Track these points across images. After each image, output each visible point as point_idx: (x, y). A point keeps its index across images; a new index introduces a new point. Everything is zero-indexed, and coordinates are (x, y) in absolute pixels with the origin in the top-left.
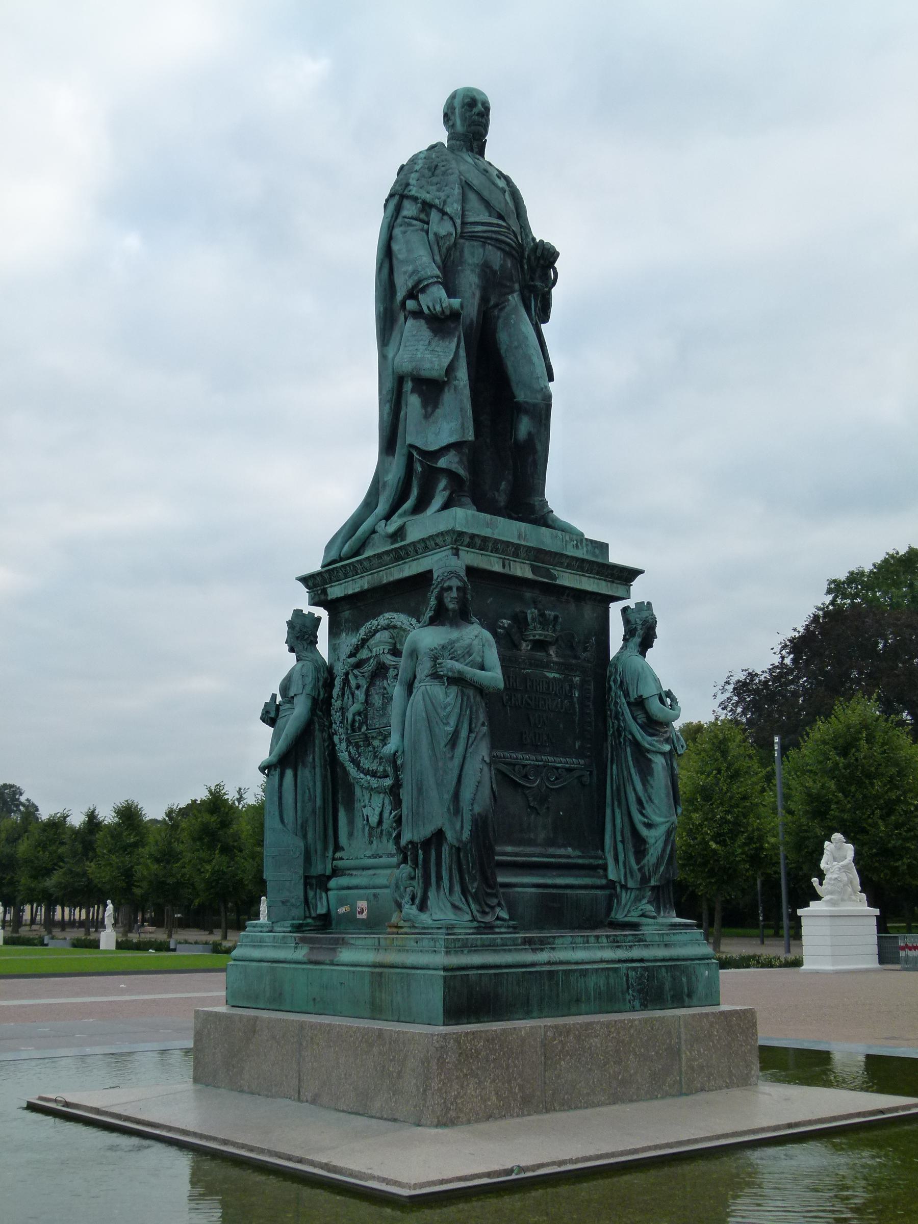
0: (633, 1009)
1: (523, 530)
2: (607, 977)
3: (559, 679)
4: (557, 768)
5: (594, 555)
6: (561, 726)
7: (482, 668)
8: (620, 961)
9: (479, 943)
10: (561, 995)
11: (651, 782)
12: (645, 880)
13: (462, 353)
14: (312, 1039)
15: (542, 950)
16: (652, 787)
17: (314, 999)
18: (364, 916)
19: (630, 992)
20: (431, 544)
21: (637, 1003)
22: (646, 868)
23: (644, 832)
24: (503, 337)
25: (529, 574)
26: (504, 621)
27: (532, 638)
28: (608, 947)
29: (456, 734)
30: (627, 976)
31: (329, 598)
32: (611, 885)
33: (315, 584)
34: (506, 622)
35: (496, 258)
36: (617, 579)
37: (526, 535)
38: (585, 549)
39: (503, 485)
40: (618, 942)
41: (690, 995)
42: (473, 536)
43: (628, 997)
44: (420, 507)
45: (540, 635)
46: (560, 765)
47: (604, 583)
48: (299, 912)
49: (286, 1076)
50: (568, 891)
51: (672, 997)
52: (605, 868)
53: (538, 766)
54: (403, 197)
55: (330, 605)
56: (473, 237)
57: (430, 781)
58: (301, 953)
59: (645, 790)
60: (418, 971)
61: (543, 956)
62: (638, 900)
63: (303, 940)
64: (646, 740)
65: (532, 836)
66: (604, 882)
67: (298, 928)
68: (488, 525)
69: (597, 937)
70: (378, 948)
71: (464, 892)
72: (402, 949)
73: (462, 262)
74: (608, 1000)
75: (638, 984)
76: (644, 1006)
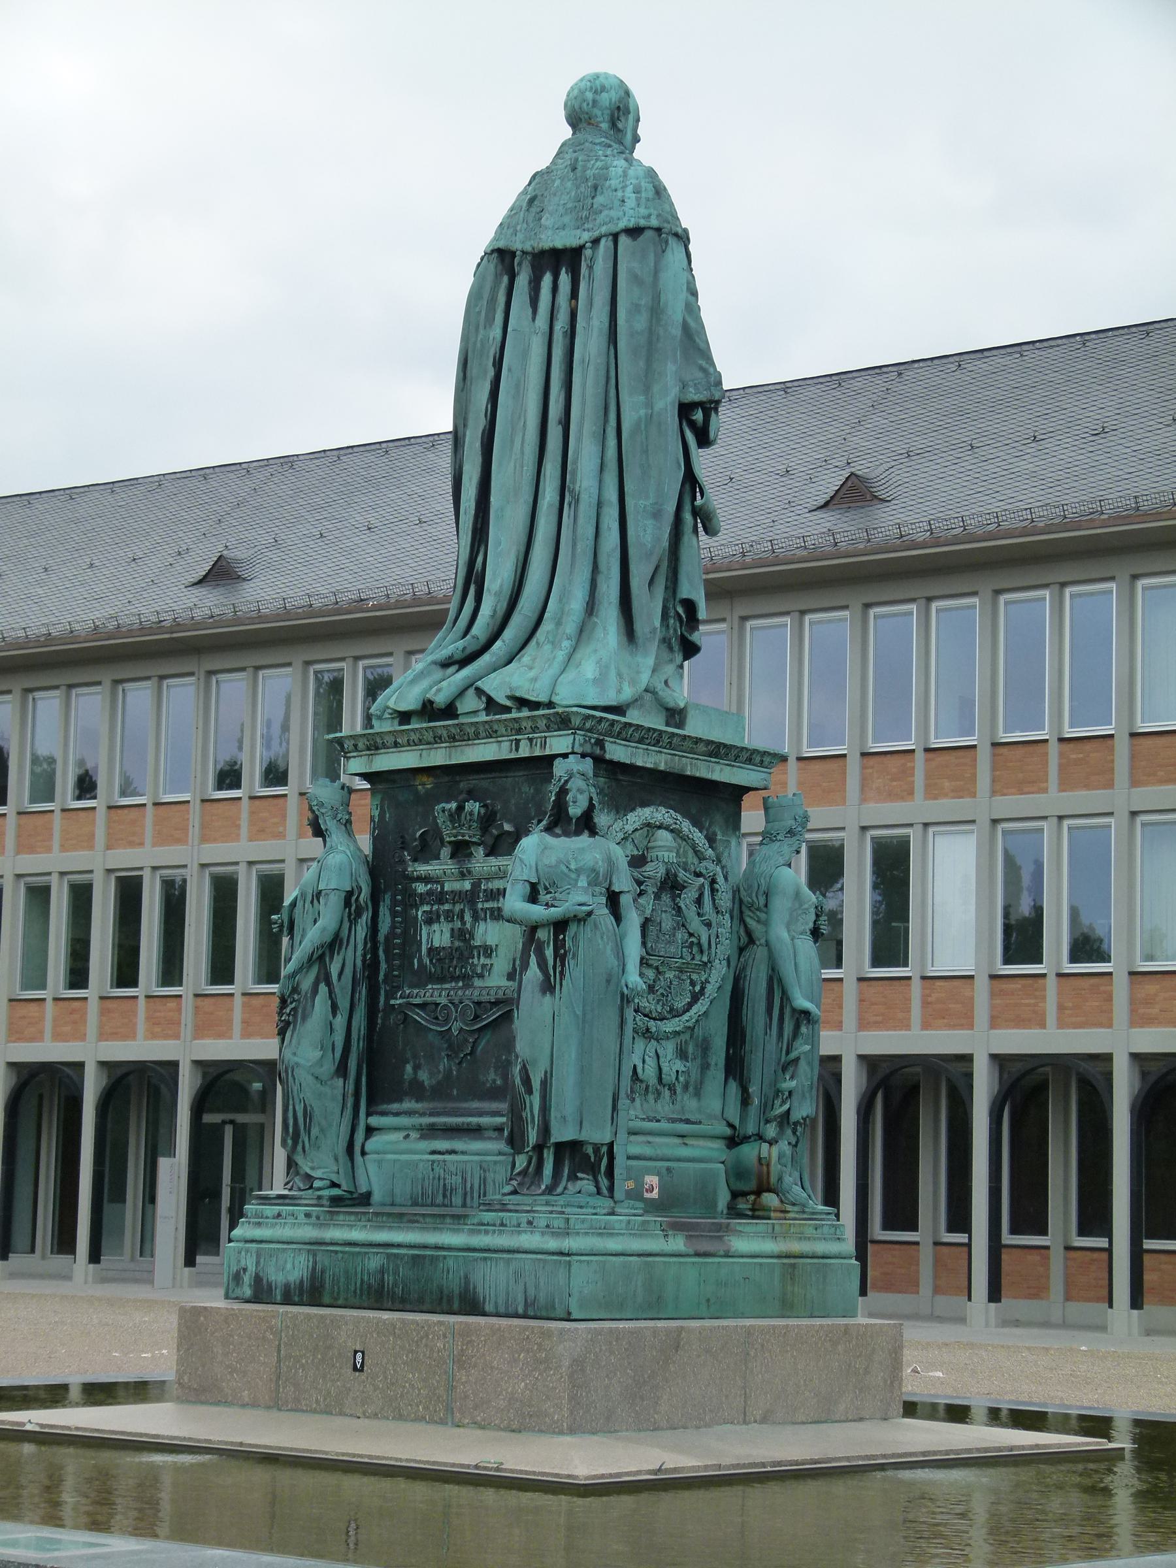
14: (763, 1346)
17: (708, 1300)
18: (655, 1194)
20: (758, 759)
31: (608, 757)
49: (727, 1396)
58: (678, 1243)
60: (832, 1261)
63: (677, 1227)
72: (802, 1238)
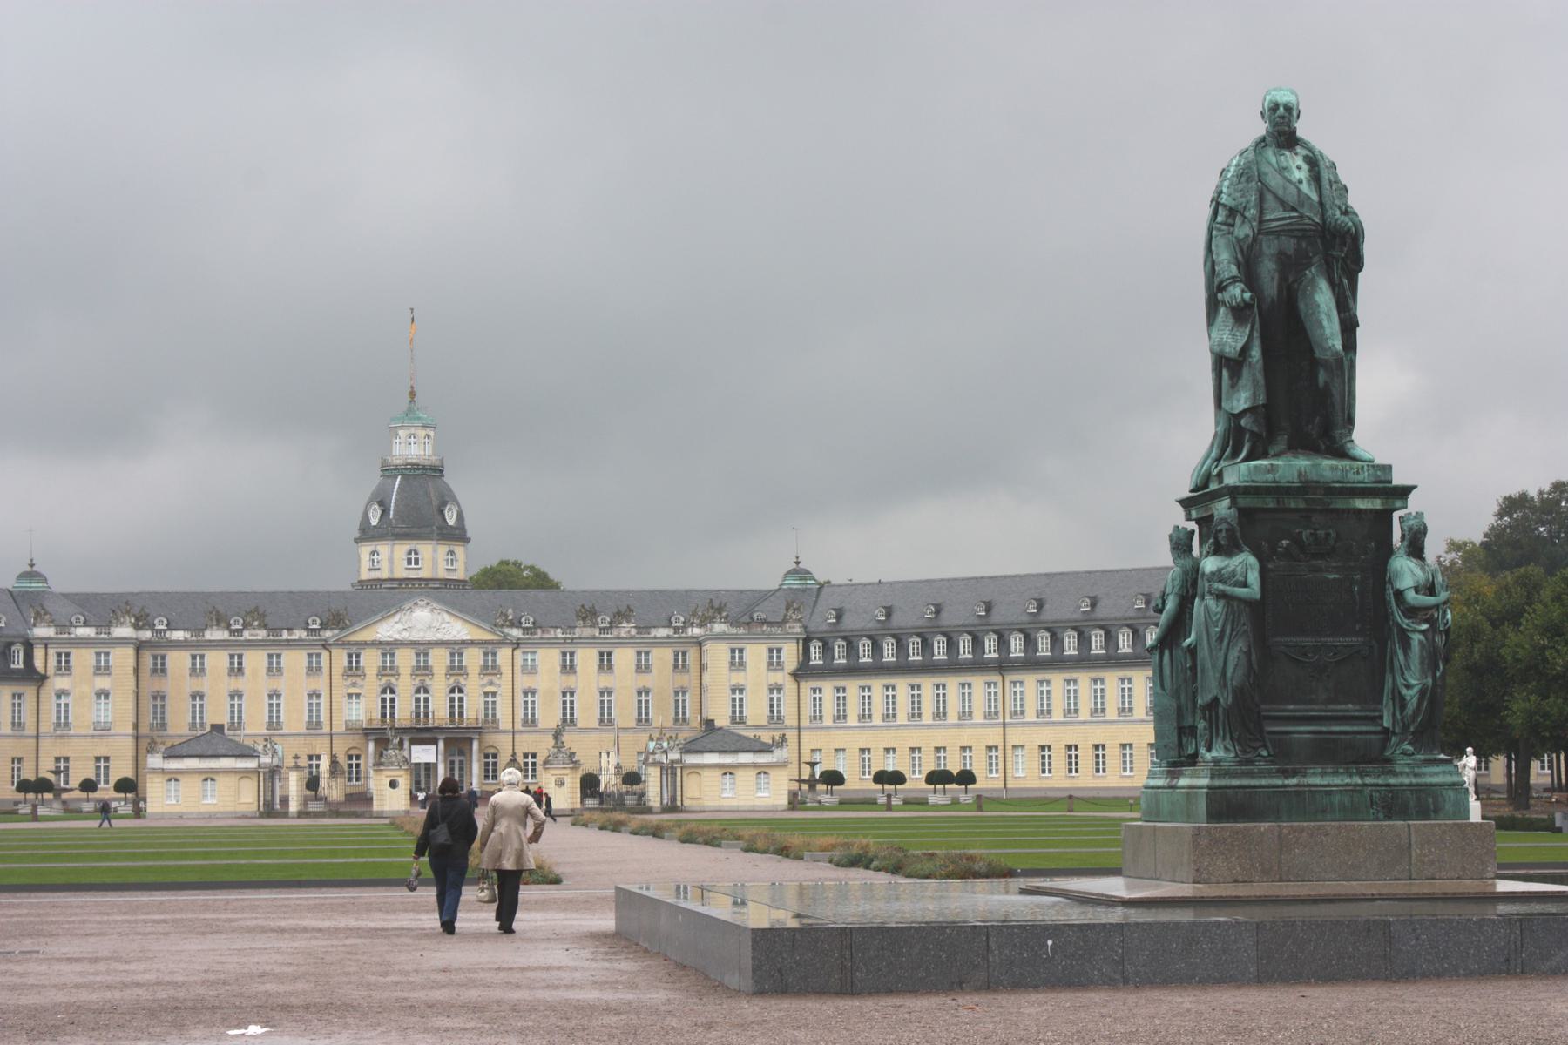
7: (1245, 585)
12: (1405, 728)
13: (1256, 334)
21: (1381, 816)
23: (1404, 691)
24: (1302, 306)
29: (1223, 632)
32: (1386, 731)
33: (1186, 503)
35: (1289, 245)
39: (1317, 420)
41: (1436, 811)
44: (1235, 454)
48: (1174, 753)
52: (1381, 717)
54: (1218, 204)
55: (1198, 521)
56: (1270, 232)
57: (1209, 665)
62: (1401, 742)
64: (1405, 623)
67: (1174, 764)
70: (1191, 776)
71: (1232, 739)
73: (1261, 253)
74: (1352, 812)
76: (1389, 818)
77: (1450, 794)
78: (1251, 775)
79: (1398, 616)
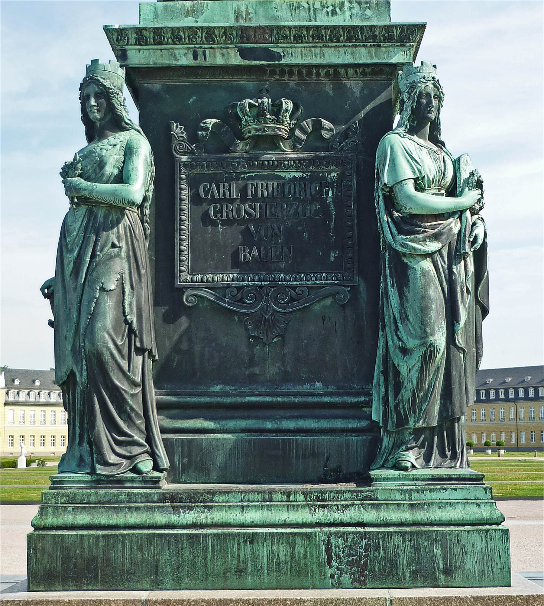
0: (340, 586)
1: (243, 9)
2: (293, 545)
3: (301, 178)
4: (294, 288)
5: (365, 17)
6: (306, 235)
8: (319, 525)
9: (92, 498)
10: (210, 563)
11: (407, 294)
15: (190, 509)
16: (407, 300)
19: (334, 563)
21: (346, 579)
22: (401, 405)
25: (236, 60)
26: (208, 121)
27: (248, 135)
28: (304, 506)
30: (329, 543)
34: (211, 122)
36: (384, 41)
37: (248, 13)
38: (348, 14)
40: (324, 500)
41: (448, 572)
42: (139, 31)
43: (329, 571)
45: (257, 130)
46: (298, 283)
47: (363, 50)
50: (300, 437)
51: (414, 573)
52: (369, 404)
53: (261, 287)
59: (402, 304)
61: (189, 517)
65: (257, 371)
66: (364, 424)
68: (188, 14)
69: (288, 494)
74: (295, 574)
75: (348, 555)
76: (360, 582)
77: (475, 541)
78: (114, 505)
79: (388, 233)
